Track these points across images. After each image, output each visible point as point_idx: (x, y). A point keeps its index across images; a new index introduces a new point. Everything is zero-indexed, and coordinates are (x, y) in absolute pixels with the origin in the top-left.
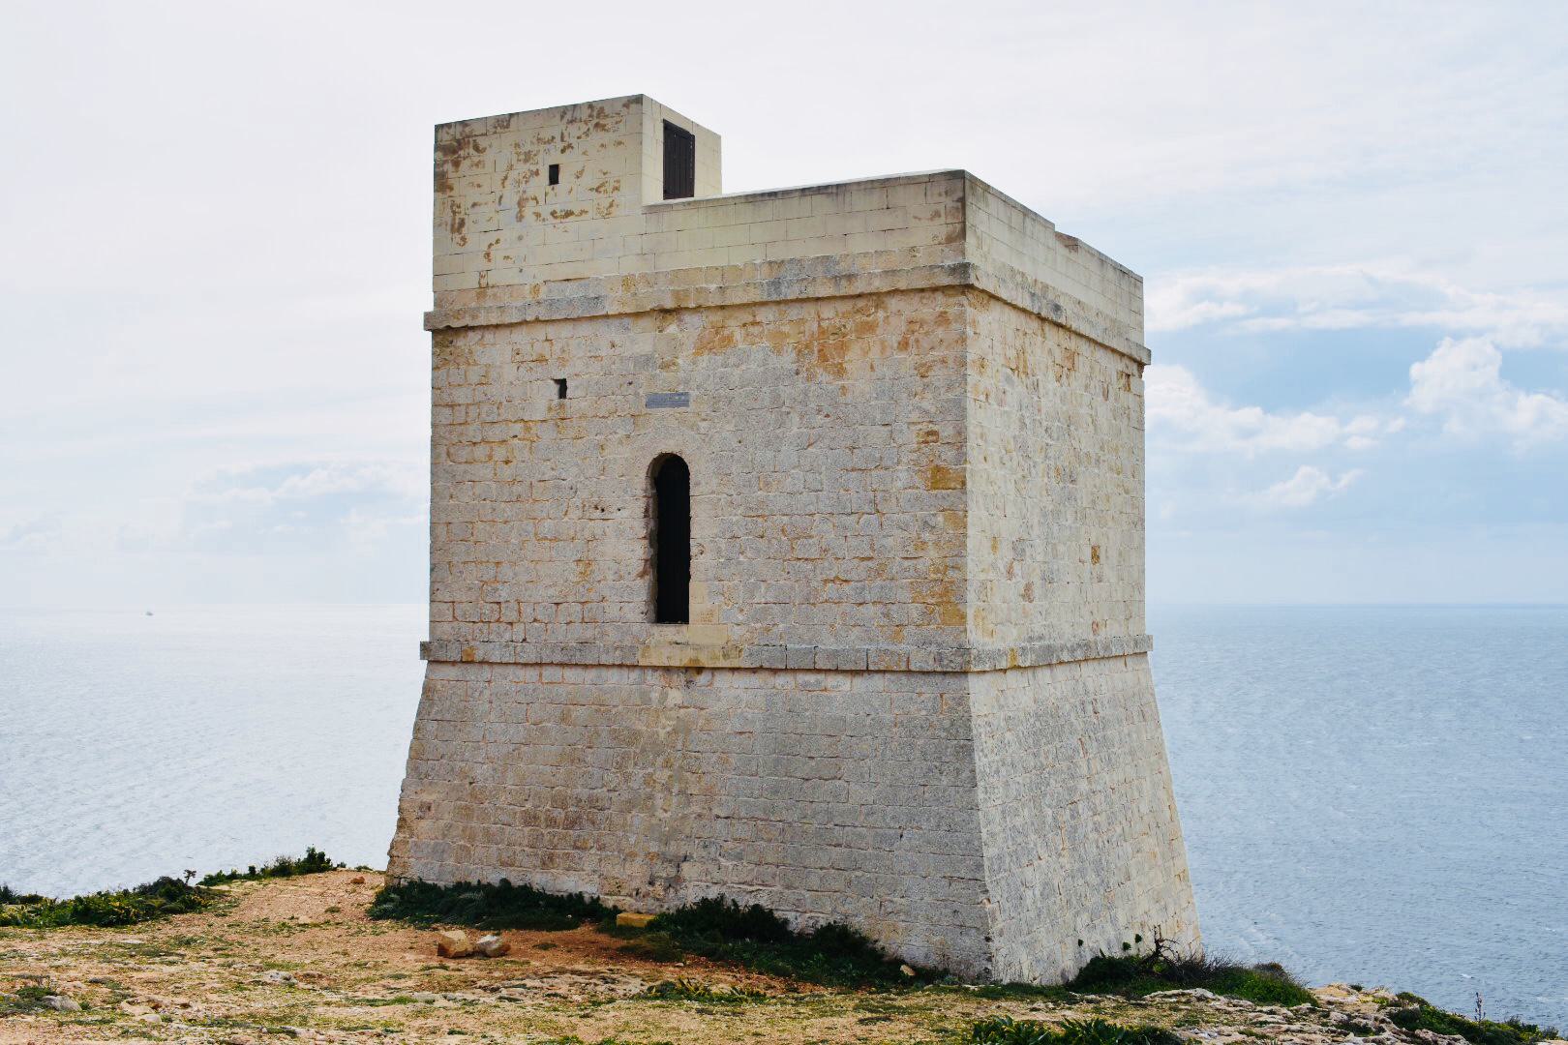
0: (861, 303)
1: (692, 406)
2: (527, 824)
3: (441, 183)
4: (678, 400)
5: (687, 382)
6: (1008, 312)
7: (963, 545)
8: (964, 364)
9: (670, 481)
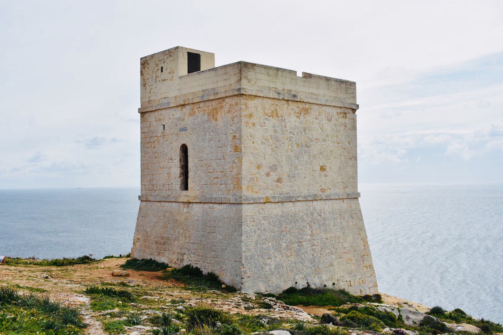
0: (220, 100)
3: (142, 74)
4: (184, 129)
5: (187, 124)
6: (268, 100)
7: (241, 168)
8: (241, 116)
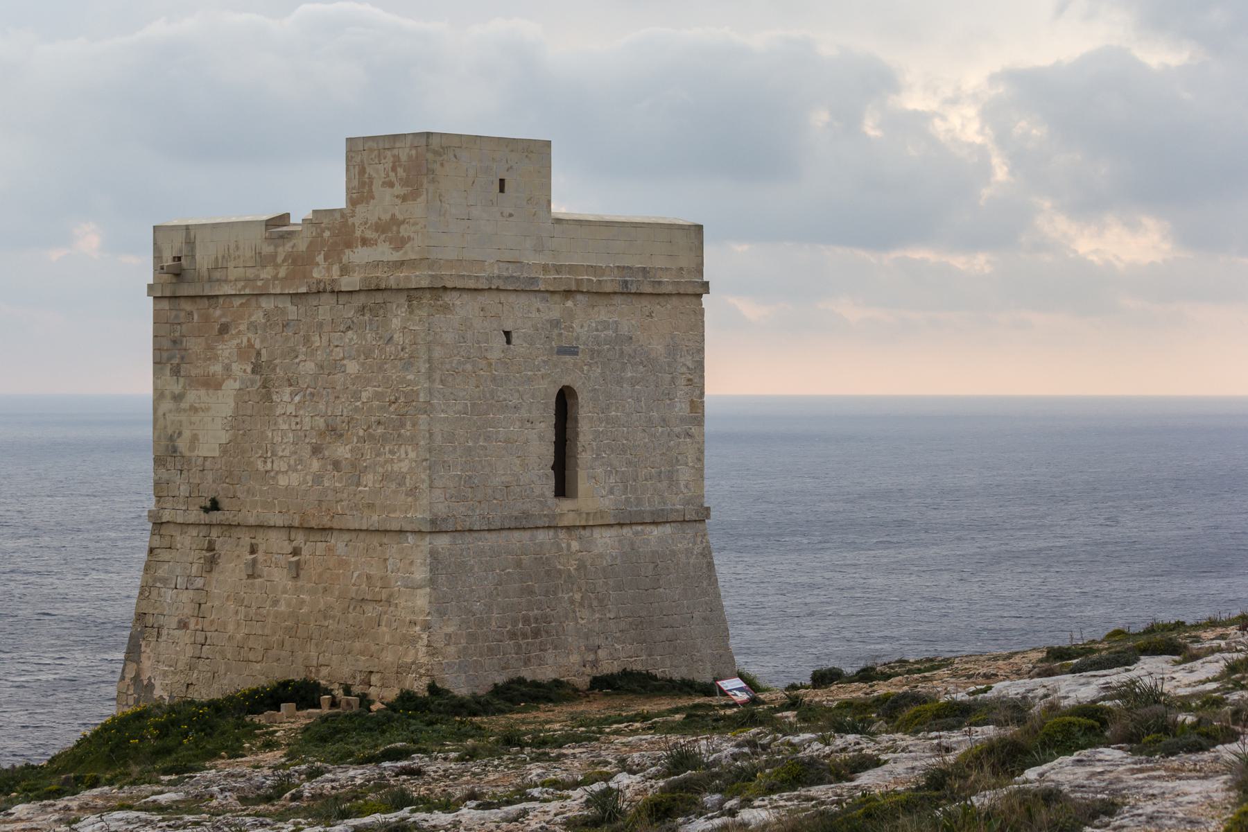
1: (581, 355)
2: (511, 639)
5: (577, 339)
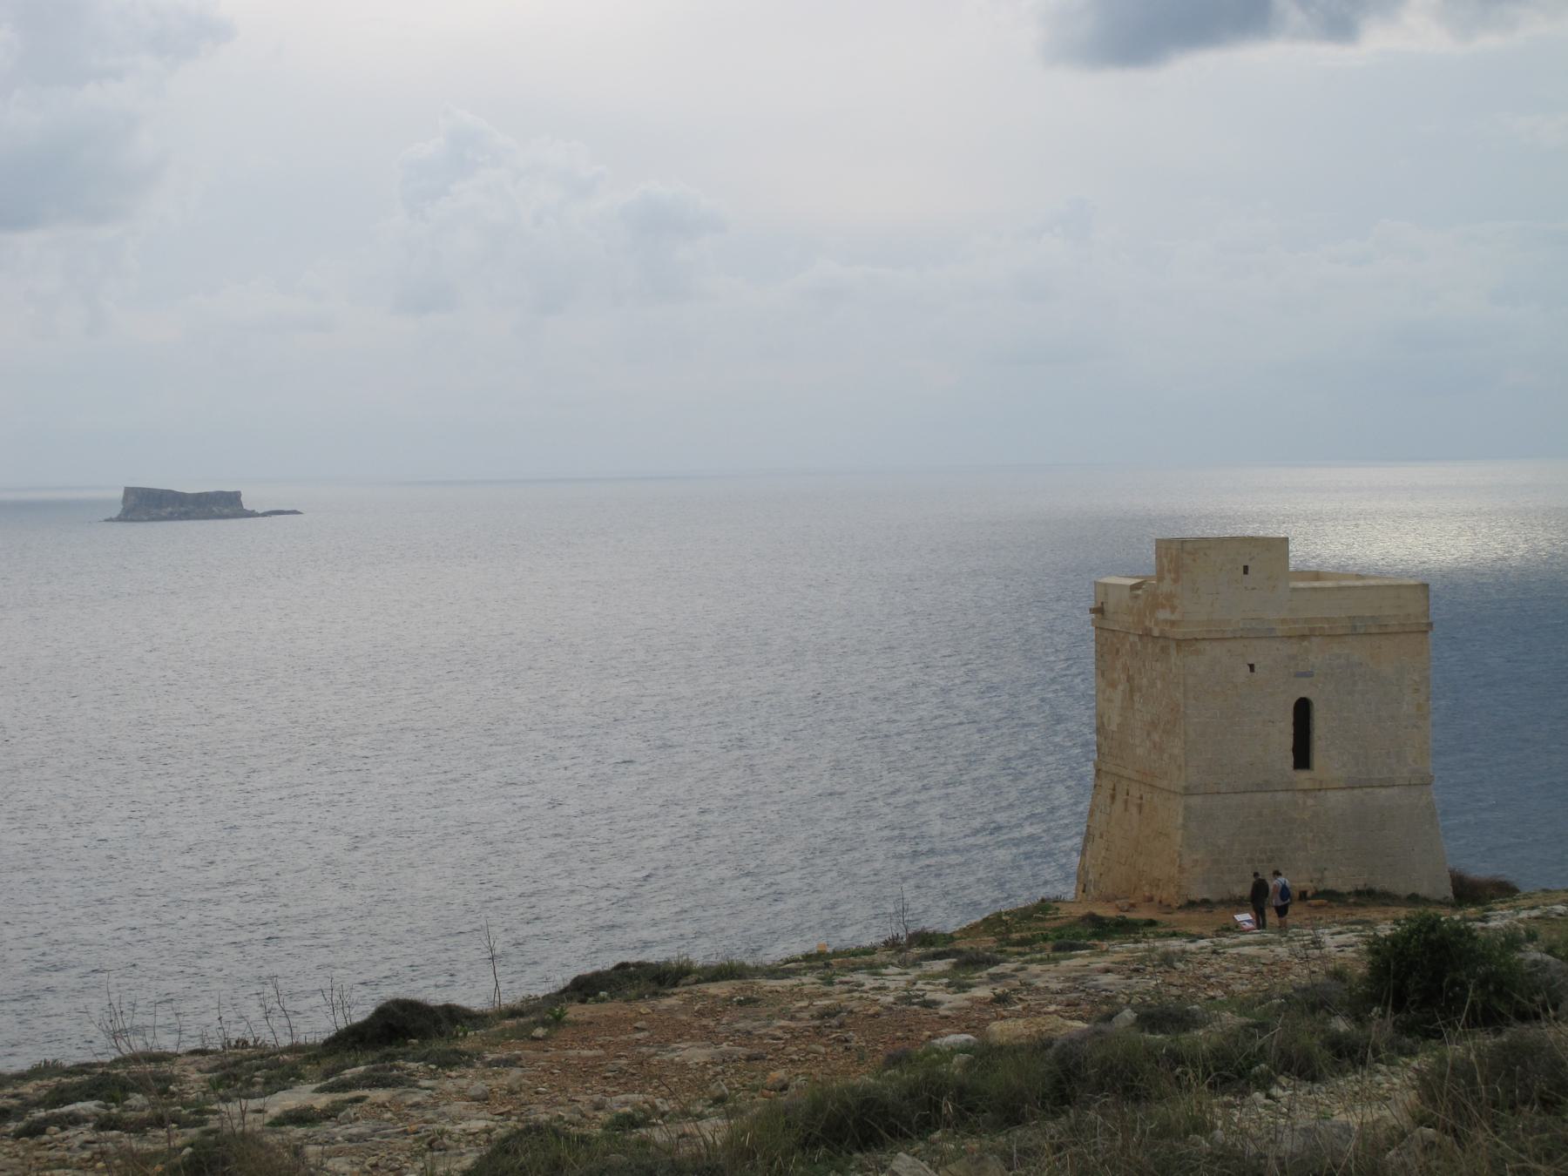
4: (1309, 675)
9: (1303, 710)
